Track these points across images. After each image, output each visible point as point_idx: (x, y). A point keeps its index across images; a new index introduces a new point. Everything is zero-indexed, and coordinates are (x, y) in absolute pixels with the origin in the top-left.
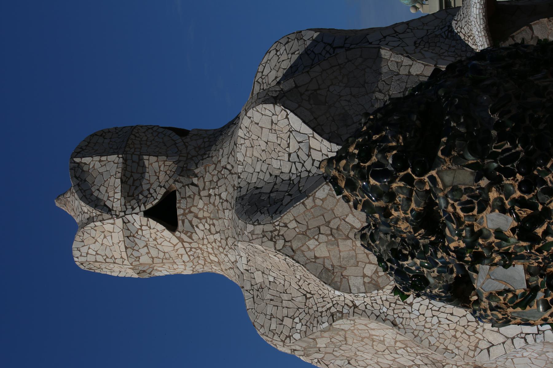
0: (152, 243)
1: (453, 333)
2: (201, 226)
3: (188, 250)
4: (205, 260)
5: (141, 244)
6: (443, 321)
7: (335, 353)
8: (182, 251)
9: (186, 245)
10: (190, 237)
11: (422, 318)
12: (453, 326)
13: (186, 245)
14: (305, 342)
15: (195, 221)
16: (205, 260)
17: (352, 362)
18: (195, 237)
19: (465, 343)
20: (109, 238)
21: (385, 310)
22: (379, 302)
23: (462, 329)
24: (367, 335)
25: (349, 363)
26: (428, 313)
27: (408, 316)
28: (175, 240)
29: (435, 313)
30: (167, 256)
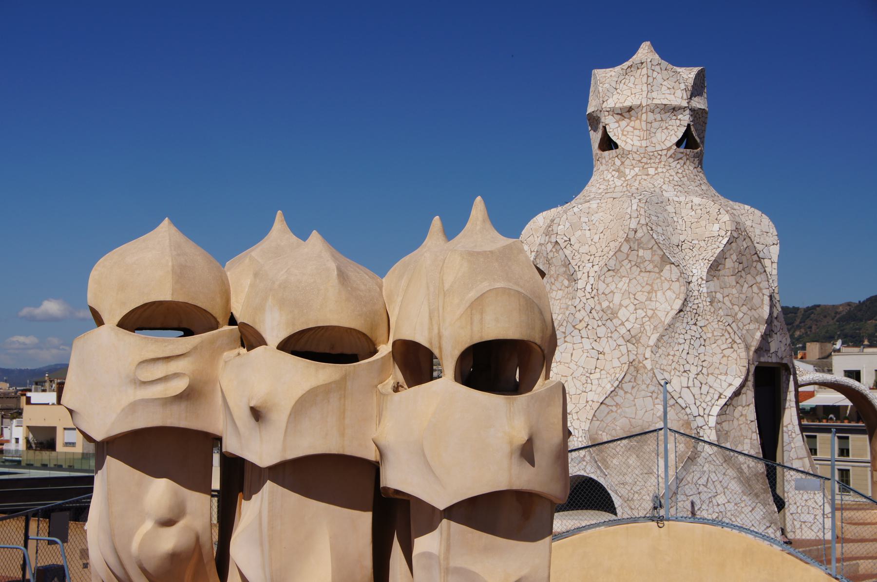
0: (664, 125)
1: (672, 353)
2: (679, 166)
3: (660, 153)
4: (646, 163)
5: (664, 116)
6: (681, 348)
7: (627, 261)
8: (658, 148)
9: (665, 152)
10: (671, 156)
11: (684, 331)
12: (678, 353)
13: (665, 152)
14: (649, 241)
15: (682, 162)
16: (646, 163)
17: (611, 273)
18: (671, 160)
19: (665, 362)
20: (668, 91)
21: (690, 305)
22: (696, 301)
23: (676, 359)
24: (655, 288)
25: (609, 270)
26: (688, 337)
27: (685, 321)
28: (669, 144)
29: (688, 342)
30: (652, 135)
